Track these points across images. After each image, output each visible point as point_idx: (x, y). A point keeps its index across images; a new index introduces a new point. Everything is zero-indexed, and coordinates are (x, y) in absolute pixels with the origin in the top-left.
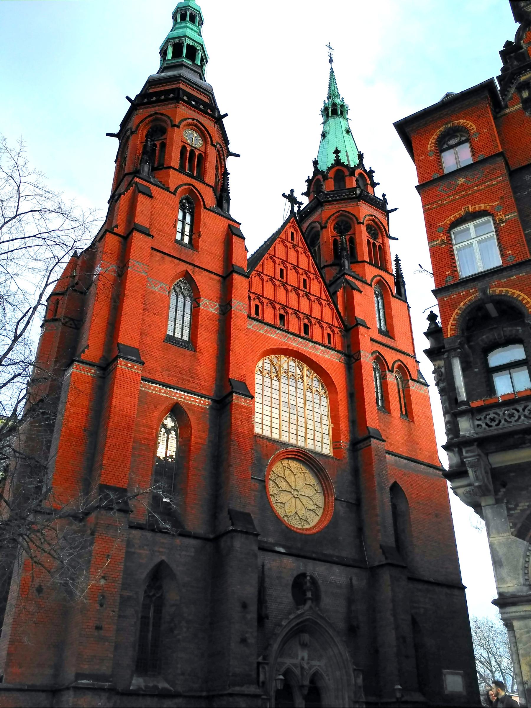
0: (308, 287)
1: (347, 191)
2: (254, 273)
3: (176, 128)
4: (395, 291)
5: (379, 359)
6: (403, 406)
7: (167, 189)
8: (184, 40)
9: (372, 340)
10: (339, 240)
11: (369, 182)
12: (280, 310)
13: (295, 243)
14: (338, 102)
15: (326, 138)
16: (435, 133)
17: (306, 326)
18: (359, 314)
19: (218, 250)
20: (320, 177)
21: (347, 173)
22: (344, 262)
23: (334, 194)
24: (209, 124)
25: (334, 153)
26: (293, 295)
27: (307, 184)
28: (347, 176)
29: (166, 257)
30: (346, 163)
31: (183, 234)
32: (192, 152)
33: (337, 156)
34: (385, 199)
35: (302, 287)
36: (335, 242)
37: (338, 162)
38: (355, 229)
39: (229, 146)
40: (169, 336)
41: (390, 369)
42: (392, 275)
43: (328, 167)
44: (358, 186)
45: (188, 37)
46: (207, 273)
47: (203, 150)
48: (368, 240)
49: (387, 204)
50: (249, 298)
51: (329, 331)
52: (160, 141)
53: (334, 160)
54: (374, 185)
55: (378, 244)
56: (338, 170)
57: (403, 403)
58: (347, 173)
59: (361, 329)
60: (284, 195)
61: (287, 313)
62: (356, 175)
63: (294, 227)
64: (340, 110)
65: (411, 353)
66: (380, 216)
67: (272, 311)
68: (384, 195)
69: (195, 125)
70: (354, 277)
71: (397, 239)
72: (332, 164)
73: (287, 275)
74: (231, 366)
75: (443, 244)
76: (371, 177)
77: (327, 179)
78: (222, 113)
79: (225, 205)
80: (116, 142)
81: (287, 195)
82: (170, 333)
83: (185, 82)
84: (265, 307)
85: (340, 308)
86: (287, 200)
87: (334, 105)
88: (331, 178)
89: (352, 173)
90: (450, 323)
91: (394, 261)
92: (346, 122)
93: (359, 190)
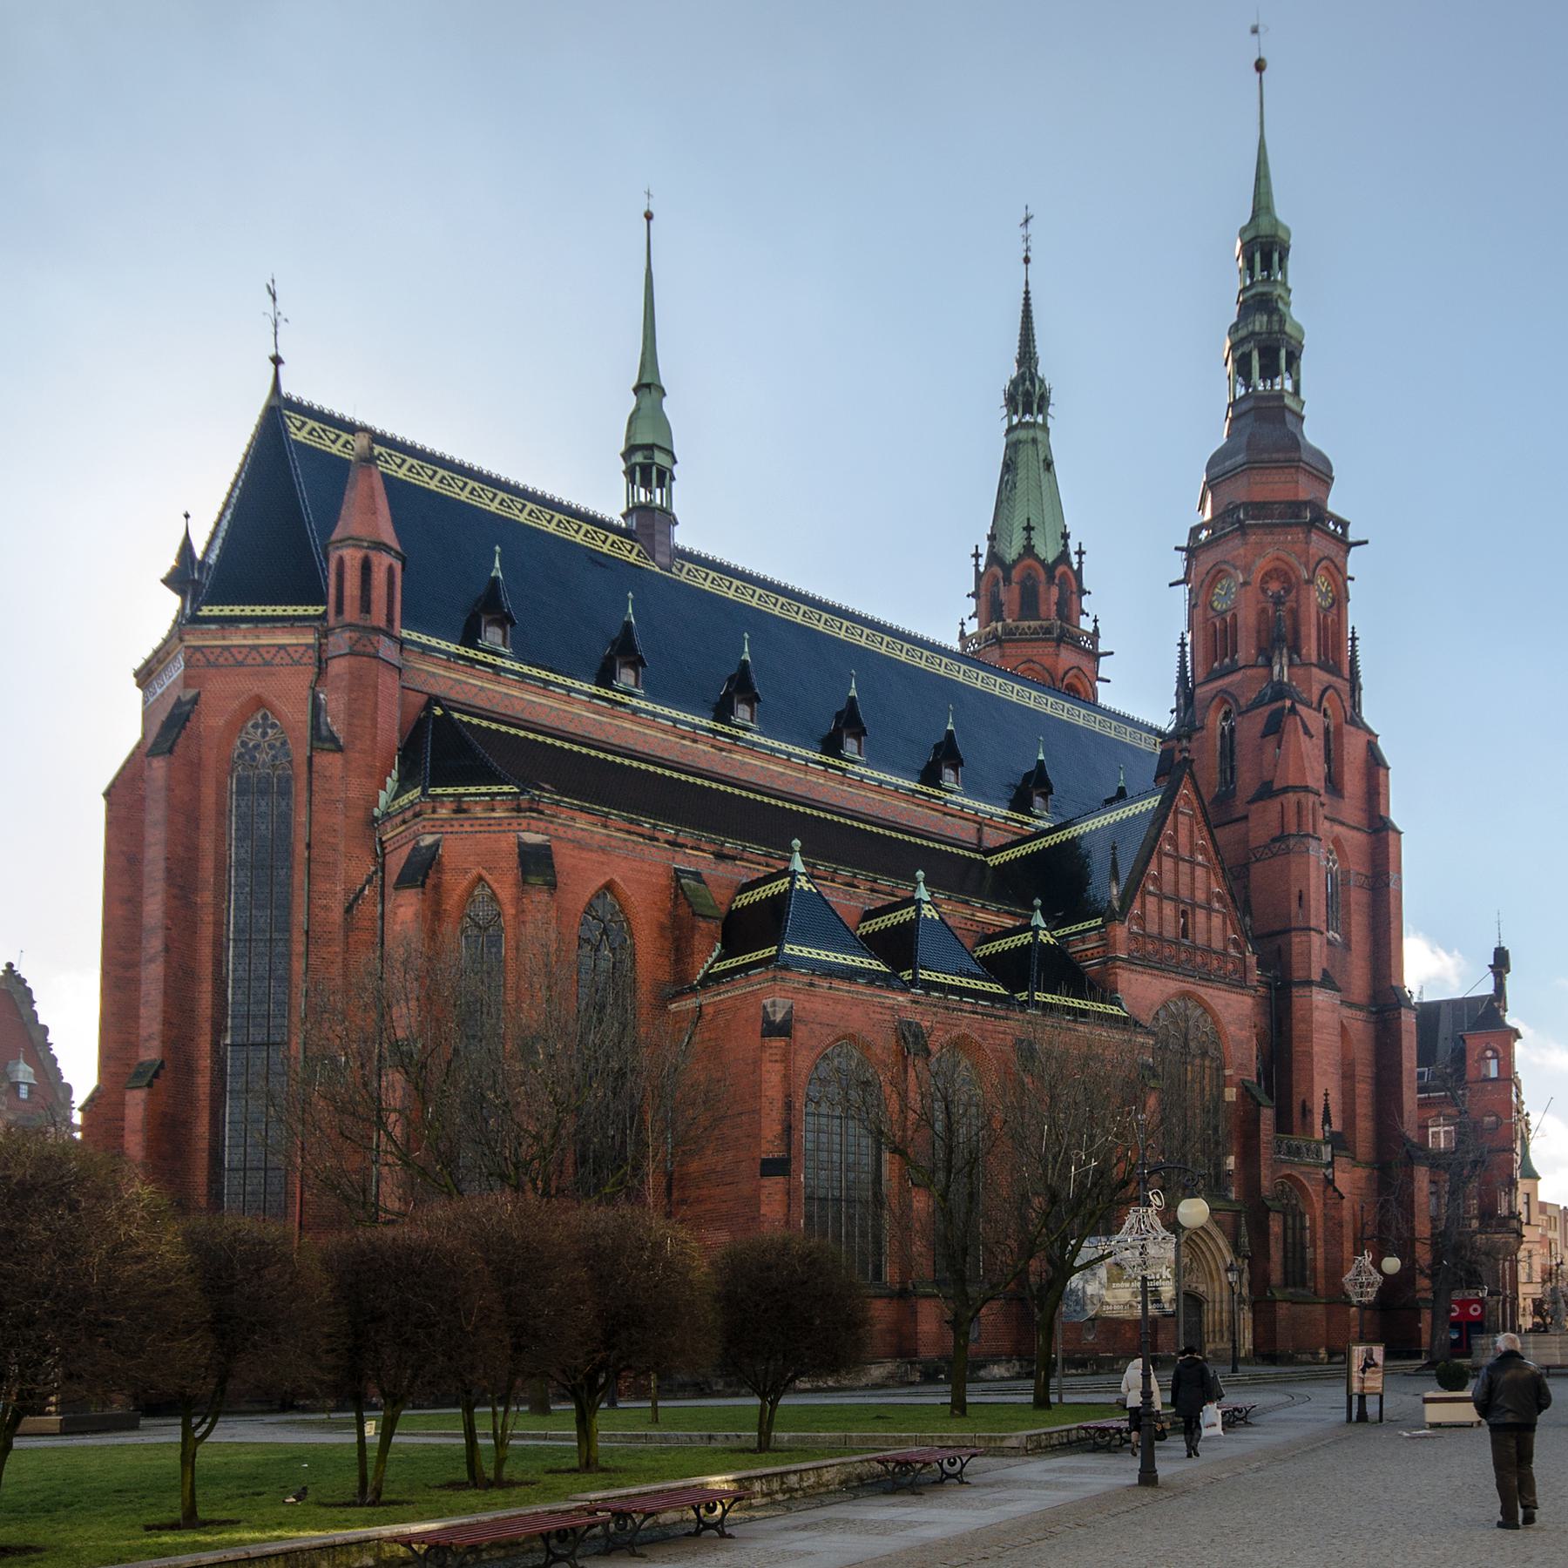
25: (1024, 529)
33: (1029, 538)
56: (1029, 567)
58: (1043, 576)
66: (1084, 663)
72: (1020, 554)
92: (1045, 435)
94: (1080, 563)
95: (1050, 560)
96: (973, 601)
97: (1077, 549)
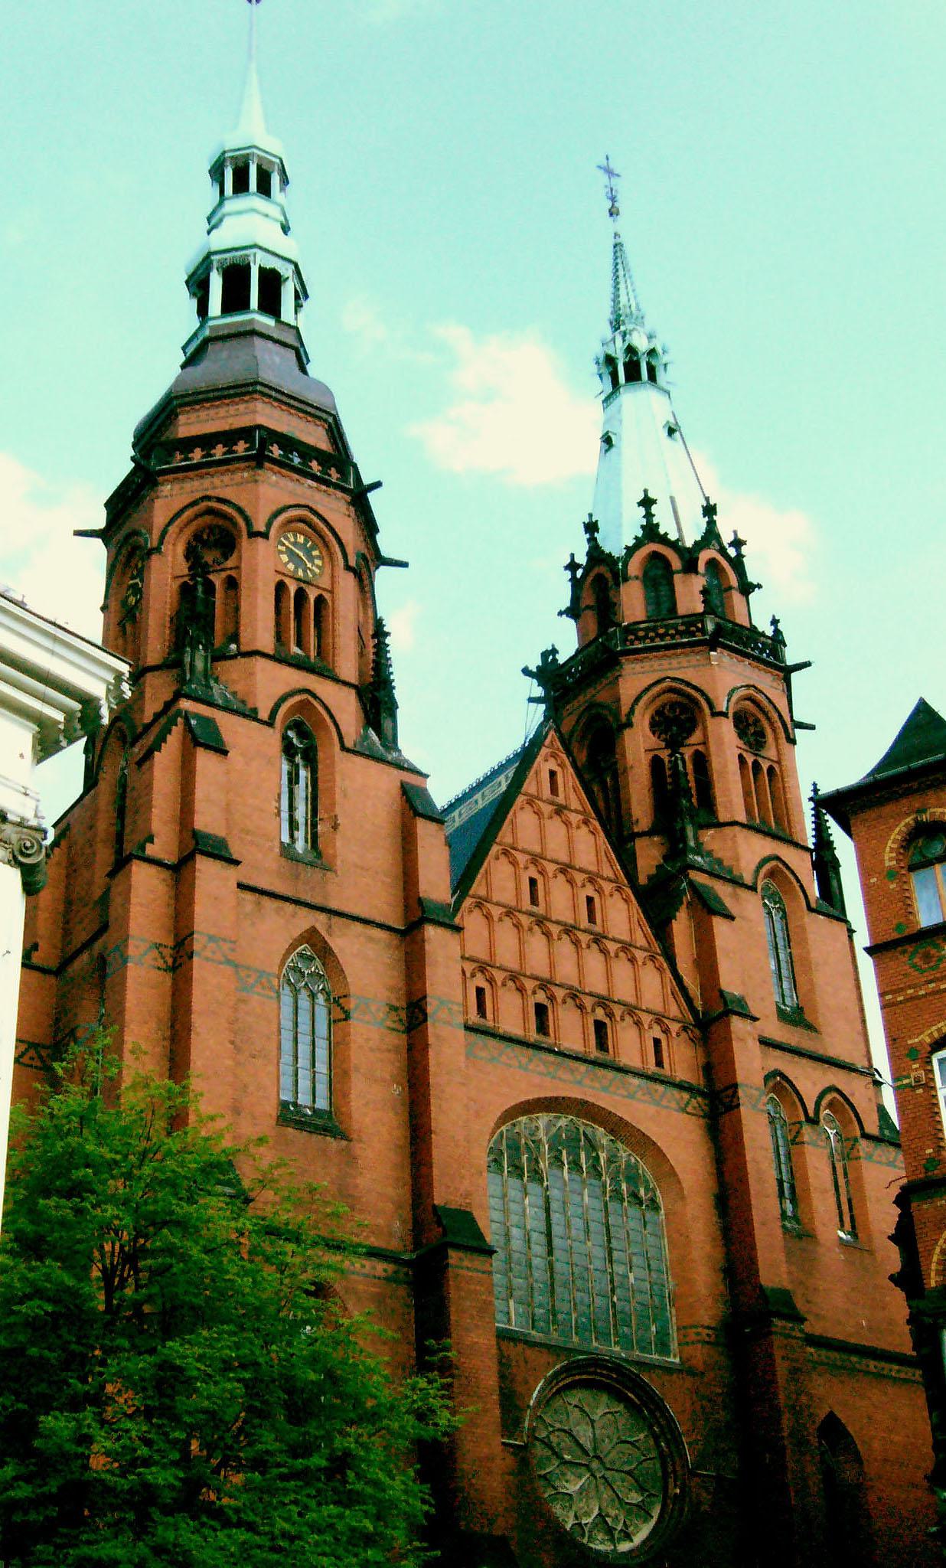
0: (598, 920)
1: (680, 621)
2: (468, 902)
3: (260, 540)
4: (815, 891)
5: (779, 1084)
6: (845, 1207)
7: (252, 715)
8: (251, 259)
9: (765, 1042)
10: (666, 760)
11: (733, 580)
12: (534, 993)
13: (561, 799)
14: (642, 344)
15: (613, 450)
16: (898, 829)
17: (600, 1027)
18: (730, 981)
19: (382, 857)
20: (603, 569)
21: (676, 563)
22: (683, 830)
23: (647, 630)
24: (335, 509)
26: (565, 947)
27: (568, 575)
28: (678, 572)
29: (268, 903)
30: (673, 536)
31: (293, 825)
32: (301, 595)
33: (649, 515)
34: (777, 632)
35: (584, 923)
36: (656, 764)
37: (651, 531)
38: (705, 729)
39: (378, 537)
40: (284, 1105)
41: (811, 1114)
42: (806, 849)
43: (627, 548)
44: (710, 609)
45: (261, 248)
46: (358, 927)
47: (325, 582)
48: (740, 756)
49: (785, 646)
50: (463, 972)
51: (656, 1032)
52: (224, 575)
53: (642, 527)
54: (747, 588)
55: (765, 765)
56: (655, 556)
57: (844, 1199)
58: (676, 563)
59: (737, 1024)
60: (526, 671)
61: (552, 998)
62: (701, 567)
63: (554, 756)
64: (649, 364)
65: (861, 1064)
66: (767, 683)
67: (517, 999)
68: (775, 622)
69: (302, 520)
70: (712, 874)
71: (812, 727)
72: (636, 538)
73: (547, 893)
74: (436, 1172)
75: (919, 1087)
76: (738, 564)
77: (626, 579)
78: (367, 480)
79: (387, 724)
80: (98, 550)
81: (535, 670)
82: (286, 1096)
83: (270, 397)
84: (501, 992)
85: (684, 966)
86: (535, 681)
87: (631, 350)
88: (637, 578)
89: (690, 567)
90: (935, 1258)
91: (811, 799)
92: (664, 398)
93: (711, 619)
94: (740, 556)
95: (689, 544)
96: (570, 624)
97: (731, 538)
